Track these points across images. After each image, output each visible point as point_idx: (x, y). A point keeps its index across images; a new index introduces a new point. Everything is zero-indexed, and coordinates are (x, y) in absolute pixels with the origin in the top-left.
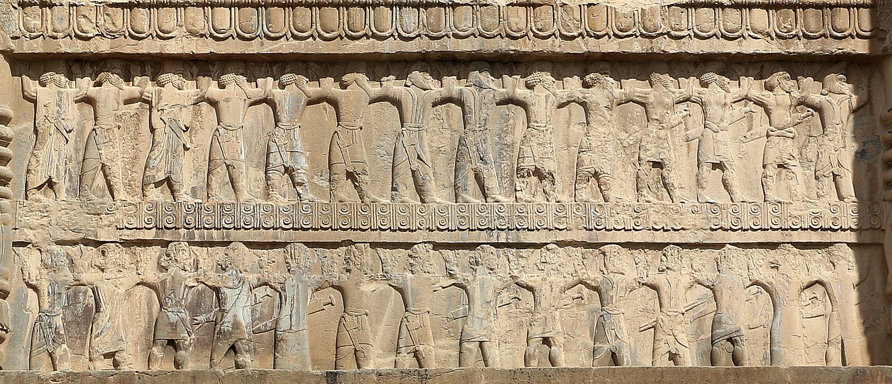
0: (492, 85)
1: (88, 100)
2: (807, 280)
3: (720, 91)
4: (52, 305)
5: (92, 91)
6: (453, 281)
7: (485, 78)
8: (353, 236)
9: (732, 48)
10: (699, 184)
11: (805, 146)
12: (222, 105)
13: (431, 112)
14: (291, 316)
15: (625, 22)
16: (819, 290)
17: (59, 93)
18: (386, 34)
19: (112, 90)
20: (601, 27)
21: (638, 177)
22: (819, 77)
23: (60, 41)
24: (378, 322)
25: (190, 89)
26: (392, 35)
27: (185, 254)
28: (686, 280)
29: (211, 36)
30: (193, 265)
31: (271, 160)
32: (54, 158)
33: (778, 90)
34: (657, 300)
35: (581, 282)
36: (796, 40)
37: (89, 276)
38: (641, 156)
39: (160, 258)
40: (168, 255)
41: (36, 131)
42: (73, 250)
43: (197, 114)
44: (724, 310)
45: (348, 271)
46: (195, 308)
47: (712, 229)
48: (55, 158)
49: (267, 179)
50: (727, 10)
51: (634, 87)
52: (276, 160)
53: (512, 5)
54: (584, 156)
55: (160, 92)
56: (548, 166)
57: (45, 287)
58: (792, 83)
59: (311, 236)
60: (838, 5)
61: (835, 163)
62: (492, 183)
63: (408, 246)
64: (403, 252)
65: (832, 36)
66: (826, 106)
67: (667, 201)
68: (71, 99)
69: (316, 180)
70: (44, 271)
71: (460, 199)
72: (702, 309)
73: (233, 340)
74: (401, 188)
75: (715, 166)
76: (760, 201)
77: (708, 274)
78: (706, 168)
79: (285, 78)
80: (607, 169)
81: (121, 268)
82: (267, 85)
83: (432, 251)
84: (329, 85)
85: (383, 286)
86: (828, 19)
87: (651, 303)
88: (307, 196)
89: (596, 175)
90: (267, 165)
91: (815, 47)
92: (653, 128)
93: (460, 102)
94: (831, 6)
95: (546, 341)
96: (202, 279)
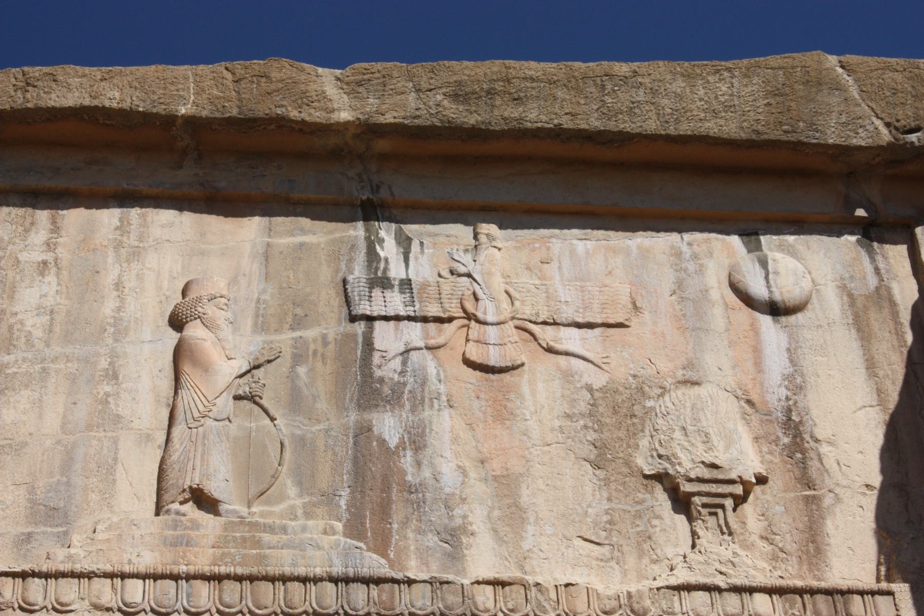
50: (725, 594)
53: (478, 583)
60: (850, 592)
94: (842, 593)
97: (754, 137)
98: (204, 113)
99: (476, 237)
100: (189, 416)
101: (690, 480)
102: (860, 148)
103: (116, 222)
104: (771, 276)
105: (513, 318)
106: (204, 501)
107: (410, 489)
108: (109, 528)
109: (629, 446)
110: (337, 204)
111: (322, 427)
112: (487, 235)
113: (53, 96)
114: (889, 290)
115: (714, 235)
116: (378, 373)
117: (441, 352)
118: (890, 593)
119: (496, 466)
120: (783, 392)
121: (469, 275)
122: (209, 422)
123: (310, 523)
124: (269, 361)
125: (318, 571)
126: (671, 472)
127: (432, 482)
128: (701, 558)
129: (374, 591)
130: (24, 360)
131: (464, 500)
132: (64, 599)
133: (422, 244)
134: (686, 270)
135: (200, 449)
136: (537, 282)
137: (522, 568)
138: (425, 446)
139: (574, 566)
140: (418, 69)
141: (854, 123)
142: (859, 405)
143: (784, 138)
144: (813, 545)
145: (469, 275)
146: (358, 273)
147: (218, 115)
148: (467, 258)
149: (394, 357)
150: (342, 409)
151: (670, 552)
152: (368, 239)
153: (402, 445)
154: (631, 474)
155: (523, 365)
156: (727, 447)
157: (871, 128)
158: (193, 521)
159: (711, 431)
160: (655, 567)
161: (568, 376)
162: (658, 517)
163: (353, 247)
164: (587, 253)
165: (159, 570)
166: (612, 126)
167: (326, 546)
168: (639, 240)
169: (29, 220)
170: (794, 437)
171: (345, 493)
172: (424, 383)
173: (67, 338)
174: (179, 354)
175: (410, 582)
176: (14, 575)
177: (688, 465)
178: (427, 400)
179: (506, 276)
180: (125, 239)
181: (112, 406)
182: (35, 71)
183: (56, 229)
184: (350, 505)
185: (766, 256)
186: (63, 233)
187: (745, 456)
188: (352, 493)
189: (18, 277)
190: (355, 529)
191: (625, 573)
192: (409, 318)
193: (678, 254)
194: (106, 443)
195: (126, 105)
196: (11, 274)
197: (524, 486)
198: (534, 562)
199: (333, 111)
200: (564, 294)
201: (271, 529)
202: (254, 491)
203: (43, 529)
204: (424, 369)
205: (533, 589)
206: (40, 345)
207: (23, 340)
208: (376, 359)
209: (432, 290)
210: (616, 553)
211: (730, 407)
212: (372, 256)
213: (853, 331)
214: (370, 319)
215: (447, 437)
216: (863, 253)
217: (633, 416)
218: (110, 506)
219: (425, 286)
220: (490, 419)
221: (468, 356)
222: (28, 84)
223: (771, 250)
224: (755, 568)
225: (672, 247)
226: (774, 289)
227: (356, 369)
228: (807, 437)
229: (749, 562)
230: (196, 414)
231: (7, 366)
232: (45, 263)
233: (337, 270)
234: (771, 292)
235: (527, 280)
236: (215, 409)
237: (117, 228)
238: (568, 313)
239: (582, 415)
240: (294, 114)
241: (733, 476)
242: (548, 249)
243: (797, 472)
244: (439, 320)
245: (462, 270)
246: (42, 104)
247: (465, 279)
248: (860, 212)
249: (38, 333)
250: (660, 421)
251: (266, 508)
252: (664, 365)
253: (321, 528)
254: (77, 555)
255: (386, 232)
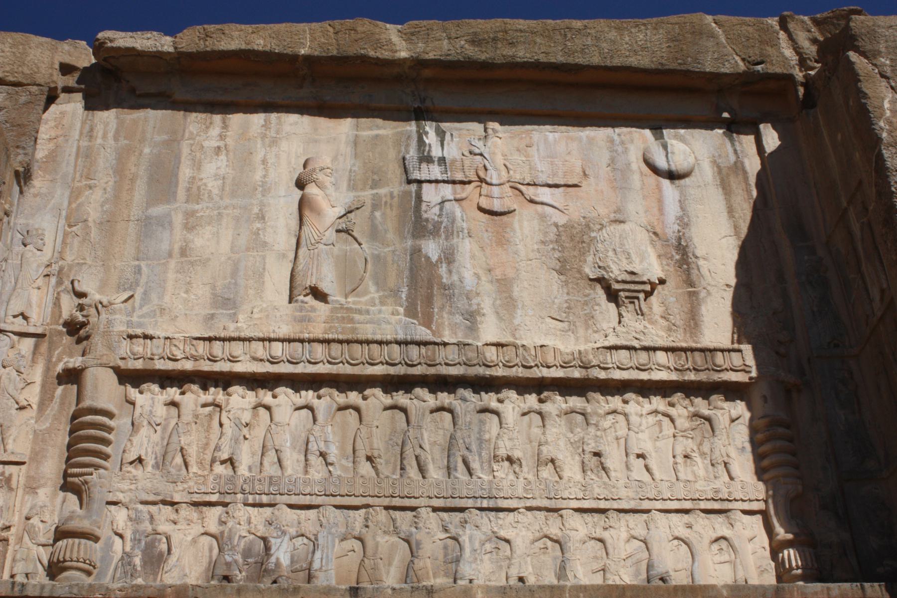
0: (473, 400)
1: (174, 404)
2: (715, 536)
3: (637, 407)
4: (133, 548)
5: (178, 398)
6: (448, 535)
7: (467, 393)
8: (370, 501)
9: (644, 376)
10: (628, 468)
11: (701, 444)
12: (274, 410)
13: (429, 417)
14: (322, 559)
15: (568, 358)
16: (724, 544)
17: (152, 398)
18: (397, 362)
19: (193, 398)
20: (550, 360)
21: (583, 462)
22: (706, 397)
23: (156, 362)
24: (390, 564)
25: (251, 397)
26: (400, 363)
27: (242, 513)
28: (624, 535)
29: (268, 360)
30: (247, 522)
31: (310, 446)
32: (145, 443)
33: (678, 406)
34: (604, 550)
35: (546, 536)
36: (688, 372)
37: (164, 527)
38: (585, 448)
39: (220, 516)
40: (227, 513)
41: (133, 424)
42: (153, 509)
43: (255, 415)
44: (654, 557)
45: (367, 526)
46: (247, 553)
47: (641, 499)
48: (146, 443)
49: (306, 460)
50: (639, 352)
51: (575, 402)
52: (313, 447)
53: (487, 345)
54: (544, 449)
55: (228, 400)
56: (517, 454)
57: (128, 535)
58: (687, 402)
59: (339, 501)
60: (715, 350)
61: (725, 455)
62: (475, 465)
63: (413, 509)
64: (409, 514)
65: (713, 370)
66: (713, 417)
67: (606, 480)
68: (161, 402)
69: (344, 462)
70: (129, 523)
71: (452, 476)
72: (638, 556)
73: (275, 576)
74: (408, 467)
75: (639, 456)
76: (674, 480)
77: (640, 532)
78: (632, 458)
79: (322, 391)
80: (560, 457)
81: (189, 522)
82: (308, 396)
83: (432, 514)
84: (354, 397)
85: (394, 539)
86: (709, 359)
87: (600, 552)
88: (336, 471)
89: (552, 461)
90: (307, 450)
91: (702, 377)
92: (592, 430)
93: (450, 411)
94: (710, 350)
95: (521, 579)
96: (253, 531)
97: (660, 67)
98: (316, 53)
99: (486, 130)
100: (308, 242)
101: (618, 282)
102: (726, 74)
103: (262, 122)
104: (669, 155)
105: (509, 181)
106: (318, 294)
107: (445, 287)
108: (261, 311)
109: (580, 261)
110: (399, 110)
111: (390, 249)
112: (493, 129)
113: (222, 43)
114: (742, 163)
115: (634, 129)
116: (425, 216)
117: (464, 203)
118: (740, 351)
119: (498, 273)
120: (676, 227)
121: (481, 155)
122: (321, 246)
123: (384, 308)
124: (358, 209)
125: (389, 337)
126: (606, 277)
127: (458, 283)
128: (624, 330)
129: (423, 350)
130: (207, 208)
131: (478, 294)
132: (235, 354)
133: (452, 135)
134: (616, 151)
135: (315, 263)
136: (524, 159)
137: (514, 336)
138: (454, 261)
139: (546, 335)
140: (449, 24)
141: (722, 58)
142: (723, 235)
143: (679, 68)
144: (693, 321)
145: (481, 155)
146: (412, 153)
147: (324, 54)
148: (480, 144)
149: (435, 206)
150: (403, 238)
151: (605, 326)
152: (418, 132)
153: (440, 260)
154: (582, 278)
155: (515, 210)
156: (641, 262)
157: (733, 62)
158: (312, 307)
159: (631, 251)
160: (596, 335)
161: (543, 217)
162: (598, 305)
163: (409, 137)
164: (555, 141)
165: (292, 337)
166: (571, 60)
167: (394, 323)
168: (588, 132)
169: (208, 121)
170: (682, 255)
171: (405, 290)
172: (453, 221)
173: (233, 194)
174: (303, 204)
175: (445, 344)
176: (204, 339)
177: (617, 272)
178: (455, 233)
179: (504, 155)
180: (268, 132)
181: (262, 236)
182: (211, 28)
183: (225, 126)
184: (408, 298)
185: (666, 143)
186: (230, 129)
187: (652, 267)
188: (409, 289)
189: (203, 157)
190: (411, 312)
191: (577, 339)
192: (444, 182)
193: (612, 141)
194: (258, 259)
195: (267, 49)
196: (198, 154)
197: (515, 286)
198: (521, 332)
199: (396, 51)
200: (540, 166)
201: (360, 312)
202: (349, 289)
203: (221, 311)
204: (454, 213)
205: (521, 349)
206: (217, 199)
207: (206, 195)
208: (424, 207)
209: (458, 164)
210: (572, 327)
211: (643, 237)
212: (421, 143)
213: (720, 189)
214: (420, 182)
215: (468, 255)
216: (727, 141)
217: (583, 242)
218: (261, 298)
219: (454, 161)
220: (494, 245)
221: (481, 205)
222: (207, 36)
223: (669, 138)
224: (657, 336)
225: (608, 137)
226: (671, 163)
227: (411, 213)
228: (690, 255)
229: (654, 332)
230: (313, 241)
231: (197, 211)
232: (219, 148)
233: (399, 152)
234: (669, 165)
235: (518, 158)
236: (324, 238)
237: (263, 126)
238: (543, 178)
239: (552, 242)
240: (372, 53)
241: (645, 279)
242: (531, 138)
243: (684, 277)
244: (463, 183)
245: (477, 151)
246: (216, 48)
247: (478, 157)
248: (726, 115)
249: (215, 191)
250: (600, 245)
251: (356, 299)
252: (603, 211)
253: (390, 311)
254: (242, 327)
255: (430, 128)
